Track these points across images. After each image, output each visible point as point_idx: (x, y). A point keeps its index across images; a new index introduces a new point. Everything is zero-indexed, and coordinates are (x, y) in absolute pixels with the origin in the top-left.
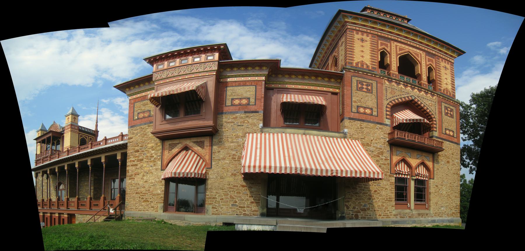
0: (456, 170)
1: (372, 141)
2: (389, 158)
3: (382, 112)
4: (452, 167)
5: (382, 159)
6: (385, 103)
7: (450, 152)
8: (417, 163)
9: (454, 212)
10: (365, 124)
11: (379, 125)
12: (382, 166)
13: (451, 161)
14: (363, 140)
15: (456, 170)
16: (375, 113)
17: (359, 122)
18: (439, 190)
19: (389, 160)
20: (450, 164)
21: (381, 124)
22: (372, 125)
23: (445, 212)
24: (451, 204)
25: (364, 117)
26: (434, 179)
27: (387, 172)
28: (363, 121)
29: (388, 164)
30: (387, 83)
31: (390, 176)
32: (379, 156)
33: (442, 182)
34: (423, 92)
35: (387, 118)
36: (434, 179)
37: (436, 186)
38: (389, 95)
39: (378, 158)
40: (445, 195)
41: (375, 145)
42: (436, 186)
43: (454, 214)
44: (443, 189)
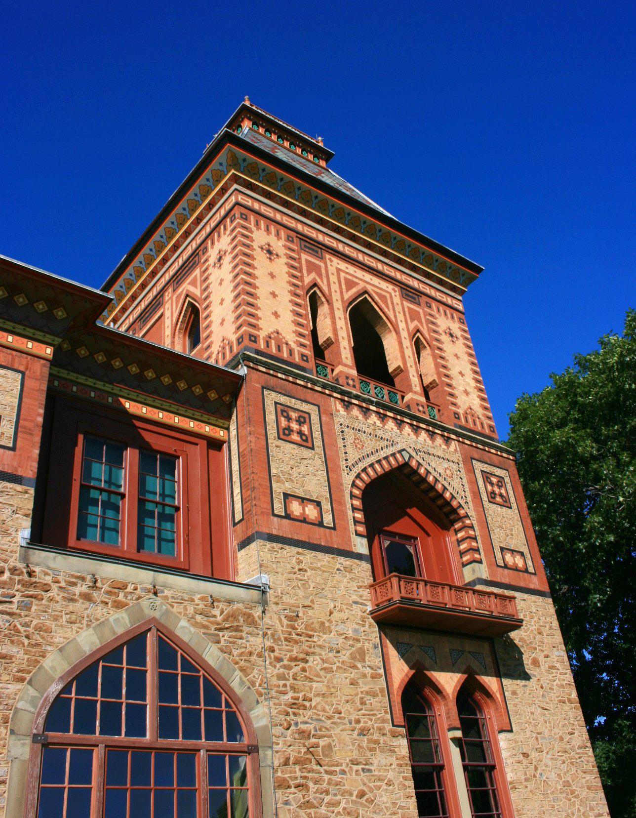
1: (331, 613)
2: (382, 671)
12: (369, 699)
14: (310, 612)
25: (302, 533)
32: (354, 667)
39: (354, 674)
41: (341, 628)
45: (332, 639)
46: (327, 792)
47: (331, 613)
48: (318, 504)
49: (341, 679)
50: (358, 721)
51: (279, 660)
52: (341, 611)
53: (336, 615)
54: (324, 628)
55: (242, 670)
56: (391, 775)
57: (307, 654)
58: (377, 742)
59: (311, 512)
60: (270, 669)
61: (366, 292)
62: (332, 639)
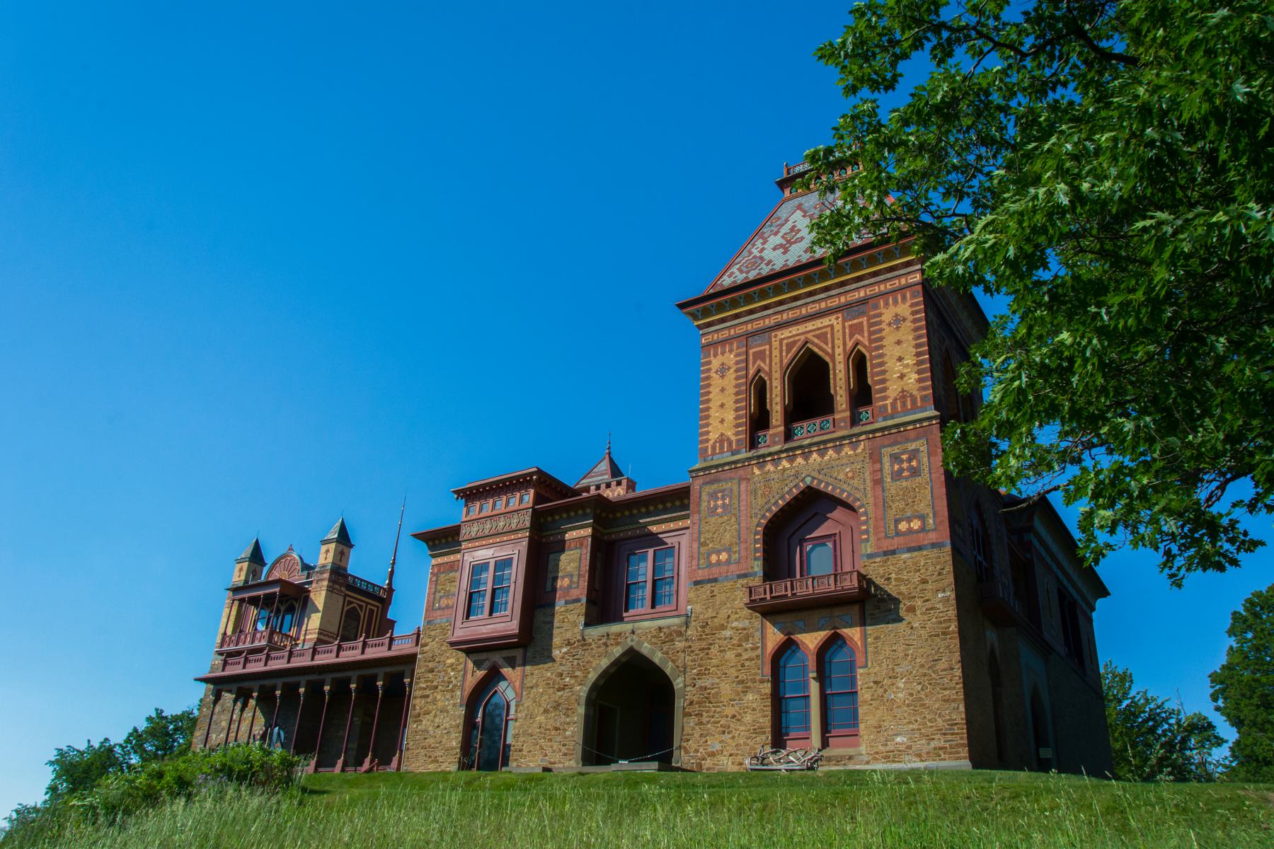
0: (940, 622)
1: (729, 617)
2: (759, 645)
4: (926, 617)
5: (746, 650)
7: (916, 578)
9: (942, 744)
10: (717, 588)
11: (740, 581)
12: (747, 663)
13: (919, 603)
14: (716, 620)
15: (940, 622)
17: (709, 585)
18: (885, 691)
19: (758, 648)
20: (918, 612)
21: (745, 576)
23: (909, 747)
24: (929, 724)
25: (715, 572)
26: (866, 666)
27: (756, 674)
28: (715, 580)
29: (758, 656)
30: (757, 471)
32: (740, 645)
33: (893, 669)
34: (831, 452)
35: (756, 559)
36: (866, 666)
37: (875, 682)
39: (740, 650)
40: (907, 702)
42: (875, 682)
43: (941, 752)
44: (898, 688)
45: (728, 633)
46: (713, 717)
47: (729, 617)
49: (730, 655)
50: (737, 677)
51: (692, 652)
52: (736, 613)
53: (733, 617)
54: (723, 627)
55: (673, 661)
56: (755, 705)
57: (711, 644)
58: (749, 687)
60: (687, 658)
62: (728, 633)
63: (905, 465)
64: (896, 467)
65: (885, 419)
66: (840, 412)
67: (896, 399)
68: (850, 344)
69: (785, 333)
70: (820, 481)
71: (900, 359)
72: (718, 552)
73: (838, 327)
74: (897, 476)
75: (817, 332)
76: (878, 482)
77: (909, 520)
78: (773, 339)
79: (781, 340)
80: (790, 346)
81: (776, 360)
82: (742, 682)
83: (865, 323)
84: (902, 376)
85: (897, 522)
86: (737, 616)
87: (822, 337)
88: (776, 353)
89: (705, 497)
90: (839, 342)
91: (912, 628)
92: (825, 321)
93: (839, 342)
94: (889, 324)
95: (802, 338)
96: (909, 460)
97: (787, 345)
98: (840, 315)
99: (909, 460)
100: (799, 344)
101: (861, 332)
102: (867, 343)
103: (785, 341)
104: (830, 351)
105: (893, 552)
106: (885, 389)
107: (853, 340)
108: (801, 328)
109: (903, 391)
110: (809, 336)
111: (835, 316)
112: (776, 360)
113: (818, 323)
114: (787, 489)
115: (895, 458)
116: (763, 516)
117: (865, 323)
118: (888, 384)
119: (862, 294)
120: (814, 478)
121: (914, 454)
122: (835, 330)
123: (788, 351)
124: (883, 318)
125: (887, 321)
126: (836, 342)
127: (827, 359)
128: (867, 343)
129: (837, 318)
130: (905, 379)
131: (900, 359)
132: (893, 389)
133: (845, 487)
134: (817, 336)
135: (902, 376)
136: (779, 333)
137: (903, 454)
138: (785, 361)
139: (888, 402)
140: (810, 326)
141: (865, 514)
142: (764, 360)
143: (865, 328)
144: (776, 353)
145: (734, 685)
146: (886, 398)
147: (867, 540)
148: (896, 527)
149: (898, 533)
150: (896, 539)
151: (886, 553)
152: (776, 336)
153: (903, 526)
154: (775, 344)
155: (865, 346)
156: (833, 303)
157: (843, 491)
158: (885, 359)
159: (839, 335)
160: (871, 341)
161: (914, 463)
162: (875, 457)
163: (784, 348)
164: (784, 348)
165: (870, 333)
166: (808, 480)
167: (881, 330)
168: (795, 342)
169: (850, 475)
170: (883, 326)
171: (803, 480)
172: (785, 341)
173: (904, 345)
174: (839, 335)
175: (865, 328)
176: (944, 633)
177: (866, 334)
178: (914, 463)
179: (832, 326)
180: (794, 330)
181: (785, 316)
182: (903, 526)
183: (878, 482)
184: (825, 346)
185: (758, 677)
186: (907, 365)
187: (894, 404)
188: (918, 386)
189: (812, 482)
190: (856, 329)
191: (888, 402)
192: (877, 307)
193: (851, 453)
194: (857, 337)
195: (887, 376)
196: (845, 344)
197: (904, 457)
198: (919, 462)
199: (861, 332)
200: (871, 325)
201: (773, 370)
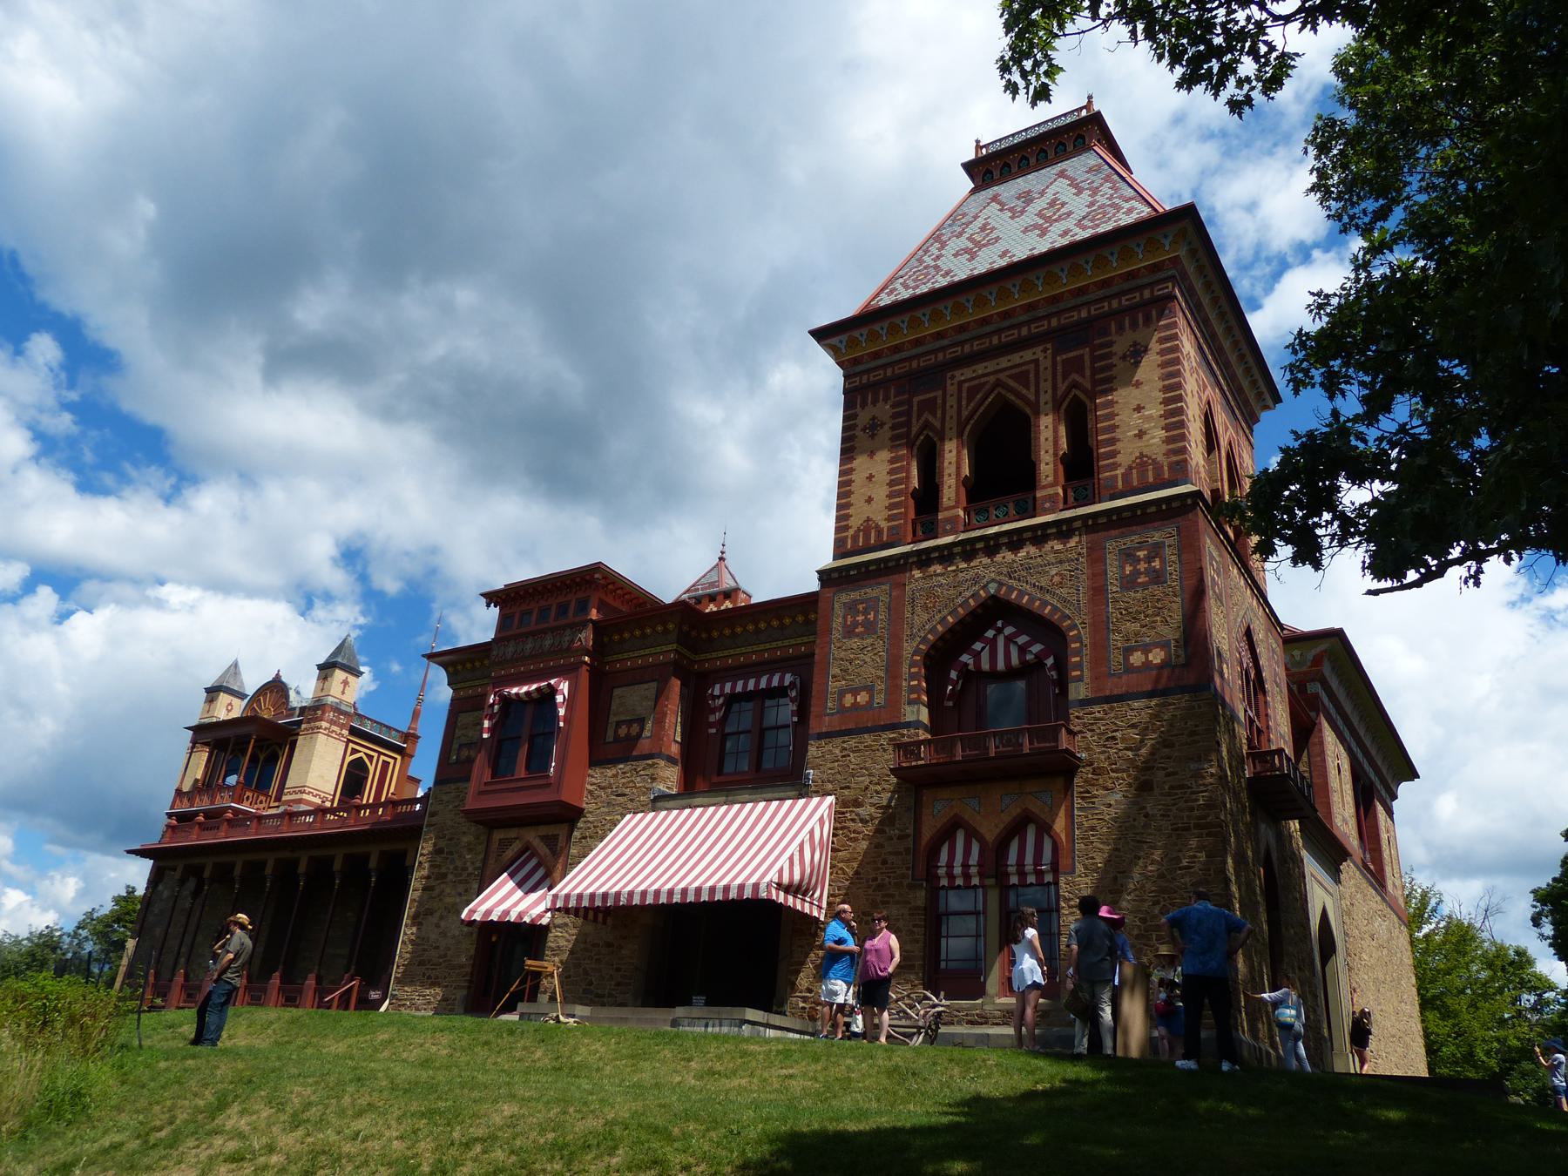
2: (910, 831)
3: (899, 687)
5: (890, 838)
6: (908, 648)
8: (1002, 826)
12: (891, 859)
16: (880, 699)
17: (839, 740)
19: (909, 836)
21: (893, 727)
22: (868, 739)
27: (904, 876)
29: (907, 849)
31: (911, 887)
33: (1115, 879)
38: (921, 617)
48: (870, 689)
50: (875, 879)
58: (892, 896)
59: (862, 698)
61: (999, 383)
63: (1142, 566)
64: (1128, 569)
65: (1113, 498)
66: (1045, 487)
67: (1130, 468)
68: (1062, 387)
69: (967, 373)
70: (1011, 588)
71: (1139, 409)
72: (855, 692)
73: (1046, 363)
74: (1129, 583)
75: (1013, 371)
76: (1098, 591)
77: (1146, 649)
78: (949, 382)
79: (960, 383)
80: (972, 392)
81: (952, 413)
82: (880, 887)
83: (1087, 358)
84: (1141, 434)
85: (1128, 651)
86: (879, 788)
87: (1022, 378)
88: (951, 401)
89: (839, 610)
90: (1046, 386)
91: (1146, 816)
92: (1028, 355)
93: (1046, 386)
94: (1124, 357)
95: (992, 379)
96: (1149, 559)
97: (969, 389)
98: (1049, 346)
99: (1149, 559)
100: (987, 387)
101: (1081, 371)
102: (1088, 386)
103: (967, 385)
104: (1032, 397)
105: (1120, 698)
106: (1114, 454)
107: (1066, 384)
108: (991, 366)
109: (1142, 455)
110: (1002, 376)
111: (1041, 348)
112: (952, 413)
113: (1016, 358)
114: (960, 600)
115: (1128, 555)
116: (924, 639)
117: (1087, 358)
118: (1119, 446)
119: (1084, 314)
120: (1001, 584)
121: (1156, 551)
122: (1041, 369)
123: (968, 405)
124: (1114, 349)
125: (1120, 354)
126: (1042, 384)
127: (1028, 411)
128: (1088, 386)
129: (1045, 351)
130: (1145, 438)
131: (1139, 409)
132: (1127, 452)
133: (1048, 597)
134: (1010, 377)
135: (1141, 434)
136: (957, 373)
137: (1140, 549)
138: (965, 413)
139: (1119, 472)
140: (1004, 362)
141: (1078, 638)
142: (934, 415)
143: (1087, 363)
144: (951, 401)
145: (870, 892)
146: (1115, 466)
147: (1080, 679)
148: (1126, 659)
149: (1129, 669)
150: (1125, 678)
151: (1108, 700)
152: (953, 377)
153: (1137, 658)
154: (951, 388)
155: (1085, 391)
156: (1044, 326)
157: (1045, 603)
158: (1116, 409)
159: (1046, 375)
160: (1095, 383)
161: (1156, 564)
162: (1096, 556)
163: (964, 395)
164: (964, 395)
165: (1094, 371)
166: (992, 589)
167: (1112, 366)
168: (982, 385)
169: (1057, 579)
170: (1115, 360)
171: (984, 587)
172: (967, 385)
173: (1145, 388)
174: (1046, 375)
175: (1087, 363)
176: (1197, 826)
177: (1088, 373)
178: (1156, 564)
179: (1036, 362)
180: (980, 369)
181: (967, 348)
182: (1137, 658)
183: (1098, 591)
184: (1024, 391)
185: (906, 882)
186: (1150, 418)
187: (1126, 476)
188: (1165, 448)
189: (999, 590)
190: (1075, 365)
191: (1119, 472)
192: (1106, 332)
193: (1060, 547)
194: (1075, 377)
195: (1118, 434)
196: (1055, 388)
197: (1141, 554)
198: (1163, 562)
199: (1081, 371)
200: (1094, 359)
201: (947, 426)
